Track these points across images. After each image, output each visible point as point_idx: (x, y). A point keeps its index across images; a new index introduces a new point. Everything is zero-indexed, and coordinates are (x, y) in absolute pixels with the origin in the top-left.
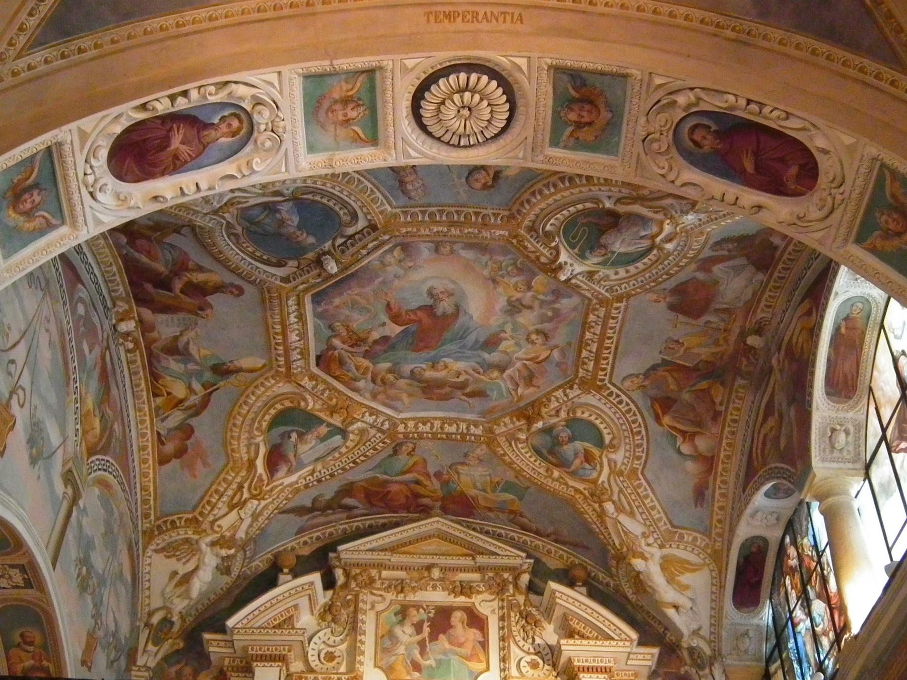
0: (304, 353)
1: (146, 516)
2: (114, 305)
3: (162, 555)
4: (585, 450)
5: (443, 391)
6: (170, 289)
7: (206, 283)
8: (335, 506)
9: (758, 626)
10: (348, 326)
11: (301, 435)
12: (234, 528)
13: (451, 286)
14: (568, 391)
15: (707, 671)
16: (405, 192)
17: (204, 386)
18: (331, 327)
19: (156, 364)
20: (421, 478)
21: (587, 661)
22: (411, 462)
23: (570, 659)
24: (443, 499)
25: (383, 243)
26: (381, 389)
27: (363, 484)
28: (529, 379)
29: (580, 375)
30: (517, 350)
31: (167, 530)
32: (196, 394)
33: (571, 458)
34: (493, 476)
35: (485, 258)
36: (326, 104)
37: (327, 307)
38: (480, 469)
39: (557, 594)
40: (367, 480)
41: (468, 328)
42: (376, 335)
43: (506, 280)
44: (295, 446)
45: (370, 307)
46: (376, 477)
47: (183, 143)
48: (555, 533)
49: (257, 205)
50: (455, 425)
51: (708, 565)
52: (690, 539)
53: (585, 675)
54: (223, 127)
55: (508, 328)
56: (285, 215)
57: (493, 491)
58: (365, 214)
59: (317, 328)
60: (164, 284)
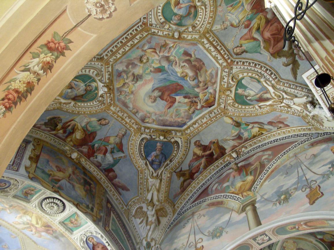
0: (211, 112)
1: (310, 129)
2: (228, 160)
3: (323, 124)
4: (175, 7)
5: (196, 63)
6: (212, 153)
7: (201, 150)
8: (291, 51)
10: (189, 109)
11: (246, 97)
12: (299, 105)
13: (146, 99)
16: (126, 133)
17: (247, 124)
18: (194, 112)
19: (249, 138)
20: (254, 30)
22: (246, 42)
25: (146, 128)
26: (209, 83)
27: (271, 50)
28: (165, 45)
29: (146, 34)
30: (155, 60)
31: (311, 124)
32: (254, 126)
34: (229, 11)
35: (127, 101)
36: (75, 225)
37: (185, 120)
38: (229, 18)
40: (268, 51)
41: (159, 81)
42: (186, 100)
43: (129, 91)
44: (253, 96)
45: (175, 111)
46: (264, 48)
47: (99, 248)
49: (153, 168)
50: (209, 48)
54: (92, 241)
55: (148, 71)
56: (153, 157)
58: (139, 138)
59: (197, 115)
60: (212, 155)
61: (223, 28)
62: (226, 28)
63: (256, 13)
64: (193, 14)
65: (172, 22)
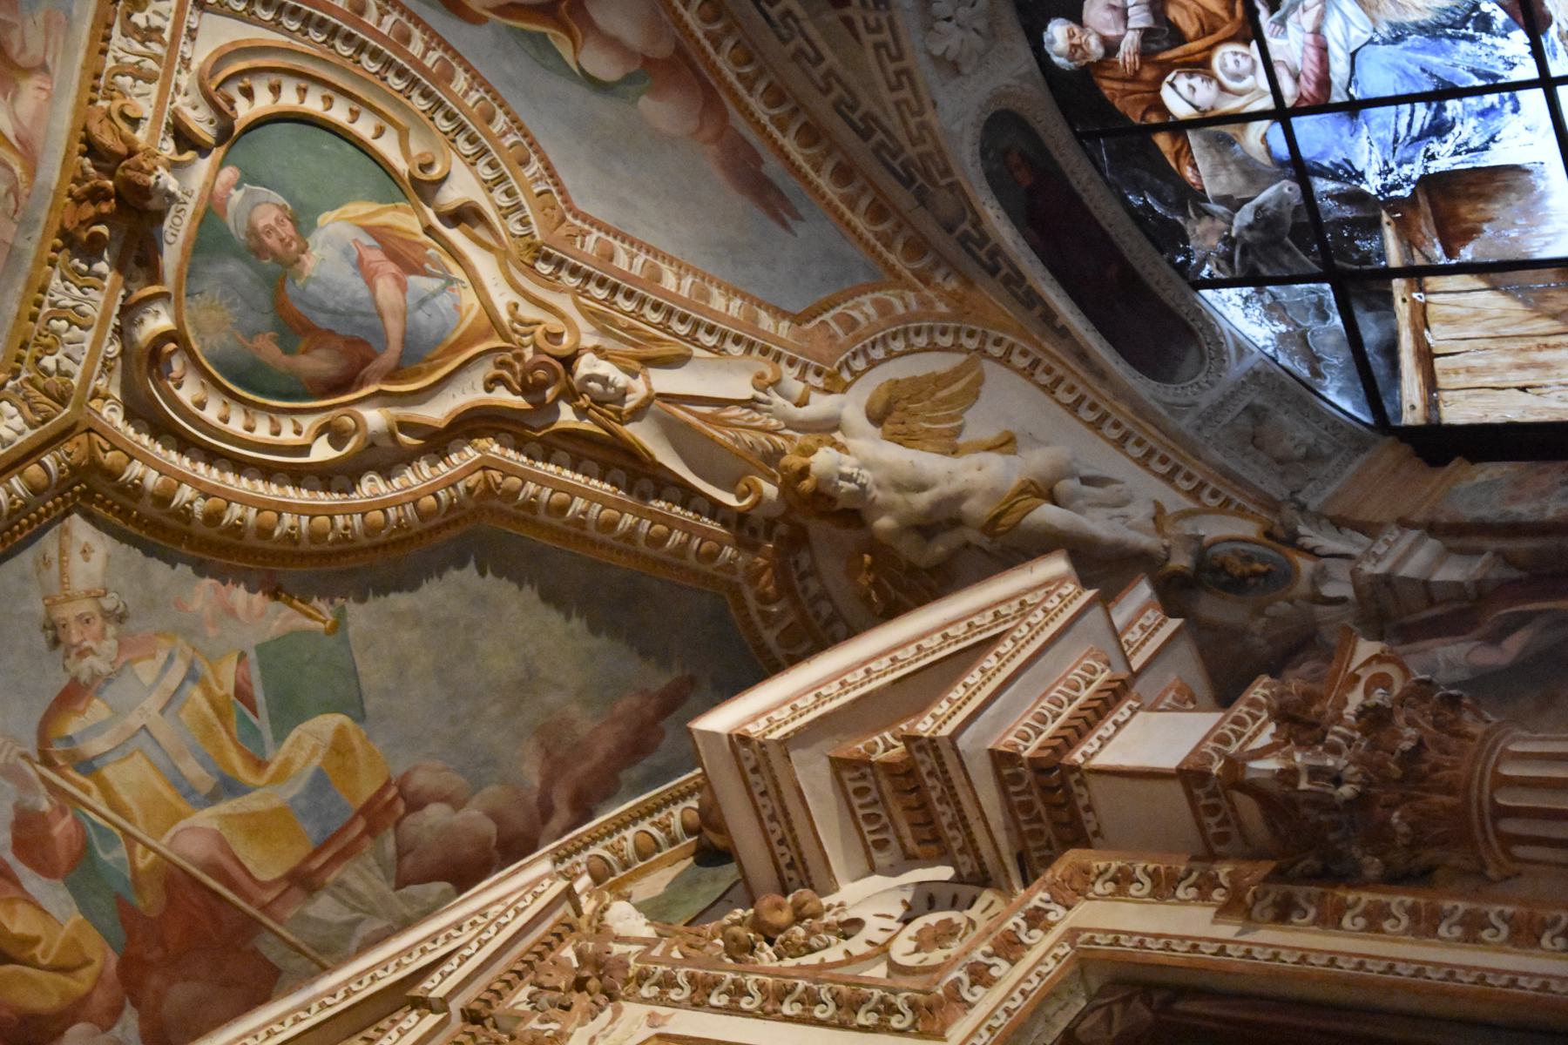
4: (370, 230)
9: (1255, 375)
14: (139, 19)
15: (1305, 565)
21: (1042, 719)
23: (1001, 760)
24: (132, 975)
33: (356, 286)
34: (204, 669)
38: (146, 671)
39: (754, 730)
48: (554, 767)
51: (983, 352)
52: (870, 310)
53: (1085, 748)
57: (260, 765)
61: (68, 612)
62: (56, 642)
63: (127, 913)
64: (286, 358)
65: (228, 174)
